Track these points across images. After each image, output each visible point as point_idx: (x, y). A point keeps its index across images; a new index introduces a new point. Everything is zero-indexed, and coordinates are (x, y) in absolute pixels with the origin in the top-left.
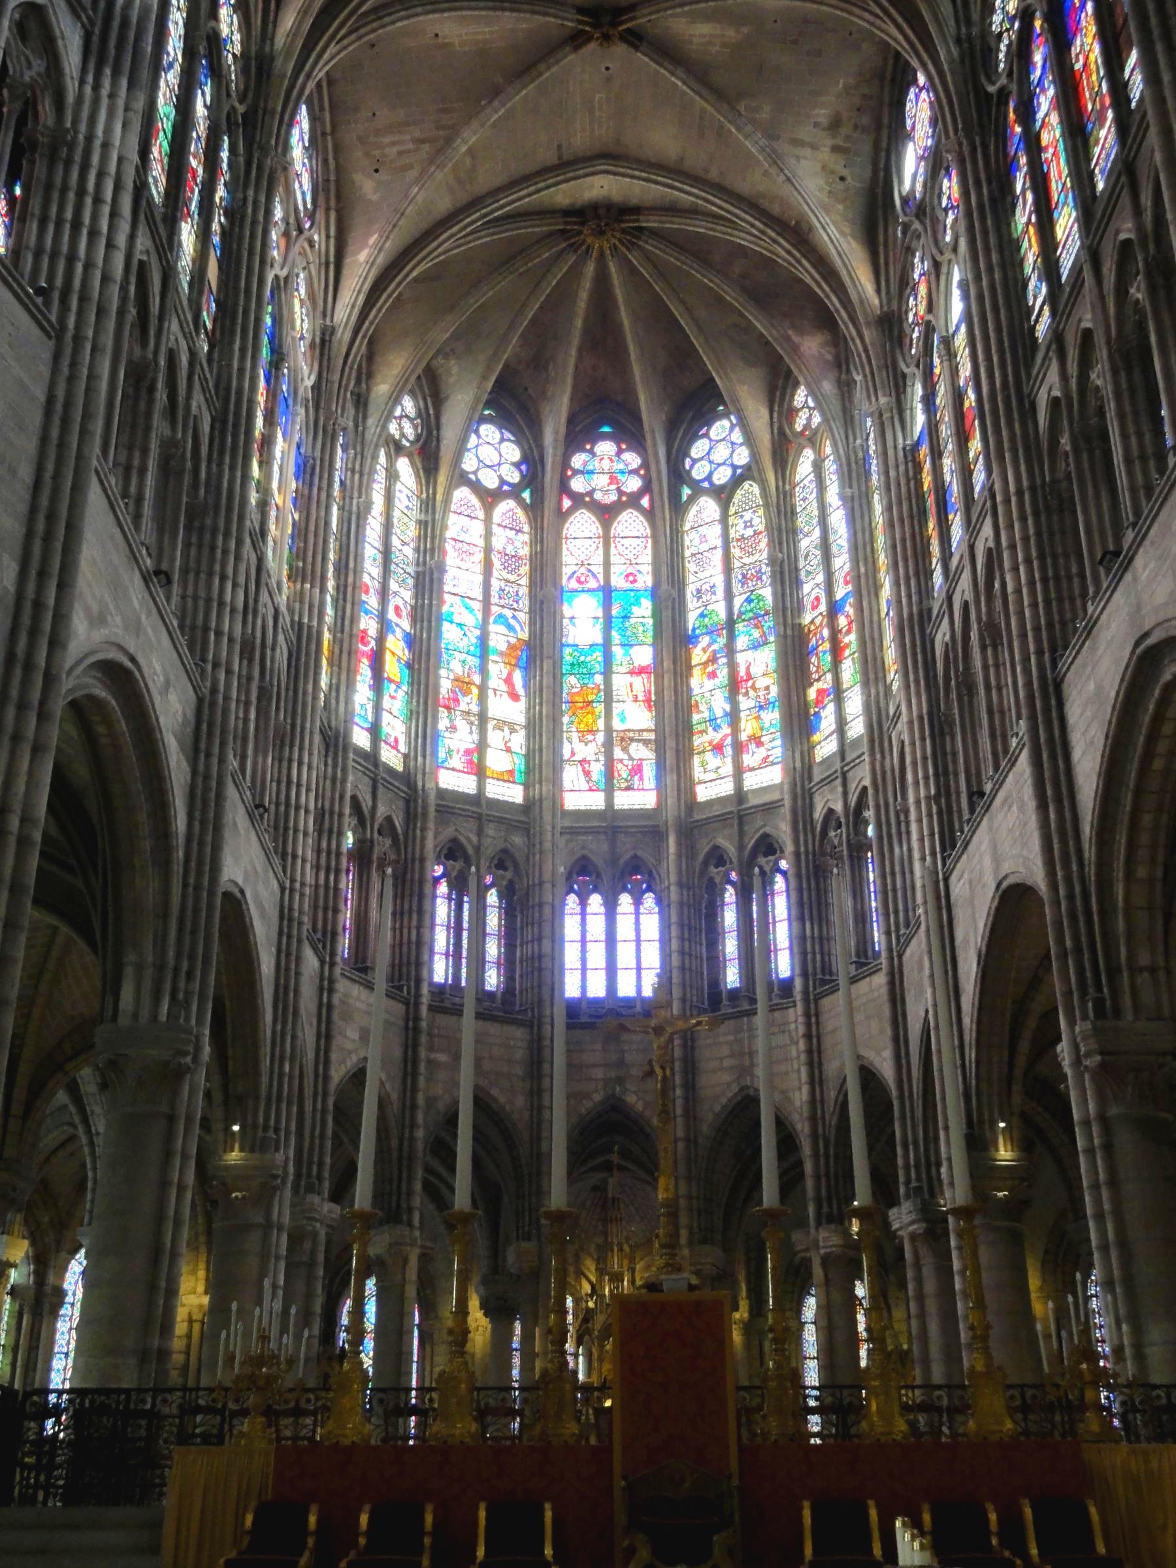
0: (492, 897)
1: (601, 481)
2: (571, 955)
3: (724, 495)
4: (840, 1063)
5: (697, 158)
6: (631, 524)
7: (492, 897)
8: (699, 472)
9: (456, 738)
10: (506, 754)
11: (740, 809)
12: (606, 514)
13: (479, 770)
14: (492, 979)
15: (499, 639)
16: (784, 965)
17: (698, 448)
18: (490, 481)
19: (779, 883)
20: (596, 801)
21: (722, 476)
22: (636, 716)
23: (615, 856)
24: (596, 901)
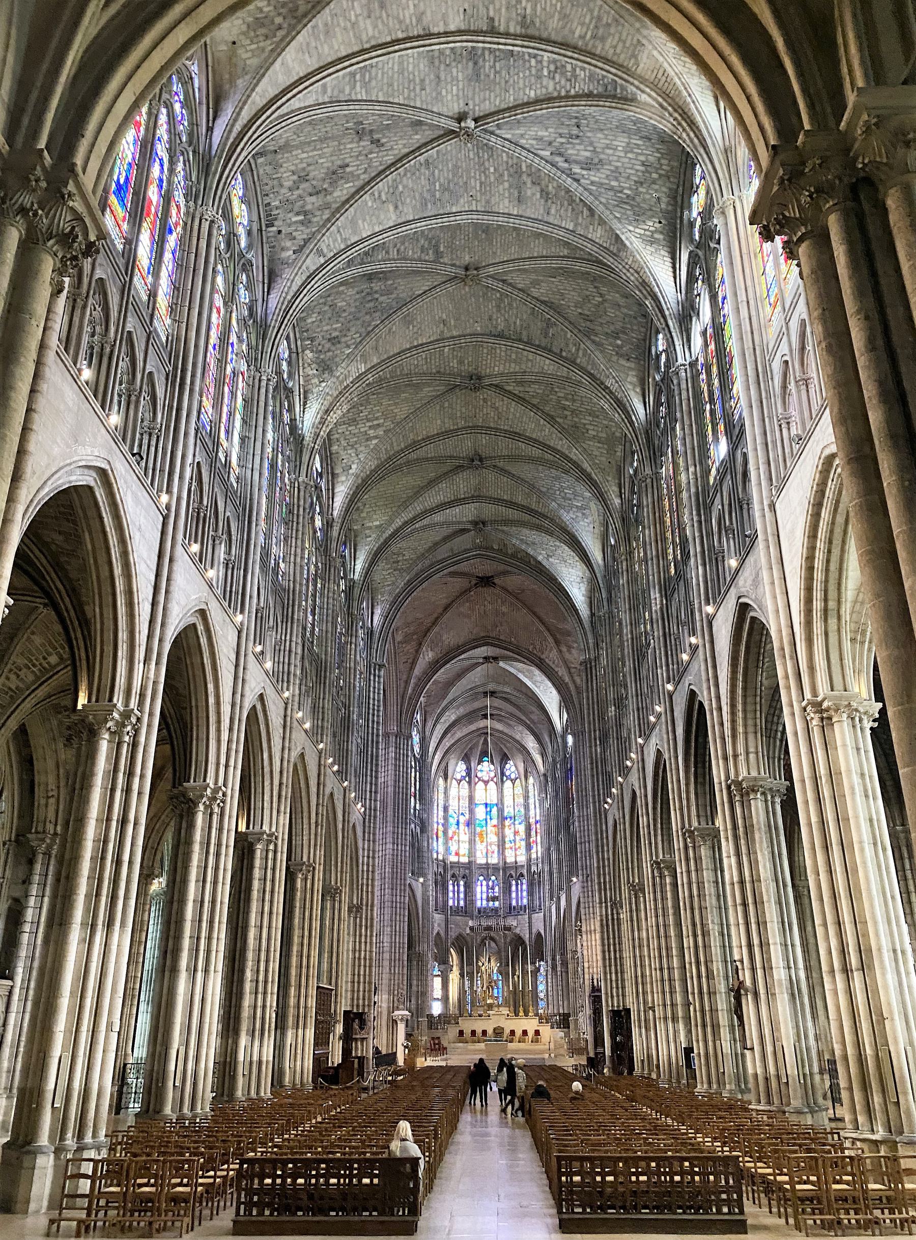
0: (462, 883)
1: (484, 773)
2: (479, 896)
3: (513, 781)
4: (534, 931)
5: (506, 730)
6: (492, 785)
7: (462, 883)
8: (508, 773)
9: (453, 848)
10: (464, 849)
11: (516, 866)
12: (486, 783)
13: (457, 854)
14: (462, 903)
15: (462, 819)
16: (525, 901)
17: (508, 766)
18: (458, 777)
19: (524, 881)
20: (483, 861)
21: (513, 776)
22: (493, 838)
23: (488, 870)
24: (484, 883)
